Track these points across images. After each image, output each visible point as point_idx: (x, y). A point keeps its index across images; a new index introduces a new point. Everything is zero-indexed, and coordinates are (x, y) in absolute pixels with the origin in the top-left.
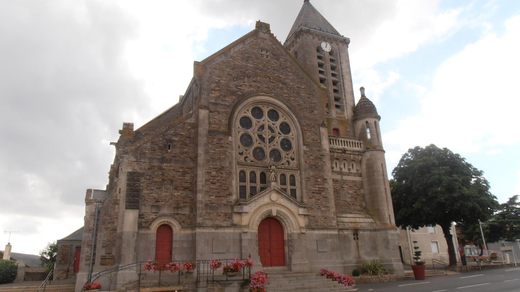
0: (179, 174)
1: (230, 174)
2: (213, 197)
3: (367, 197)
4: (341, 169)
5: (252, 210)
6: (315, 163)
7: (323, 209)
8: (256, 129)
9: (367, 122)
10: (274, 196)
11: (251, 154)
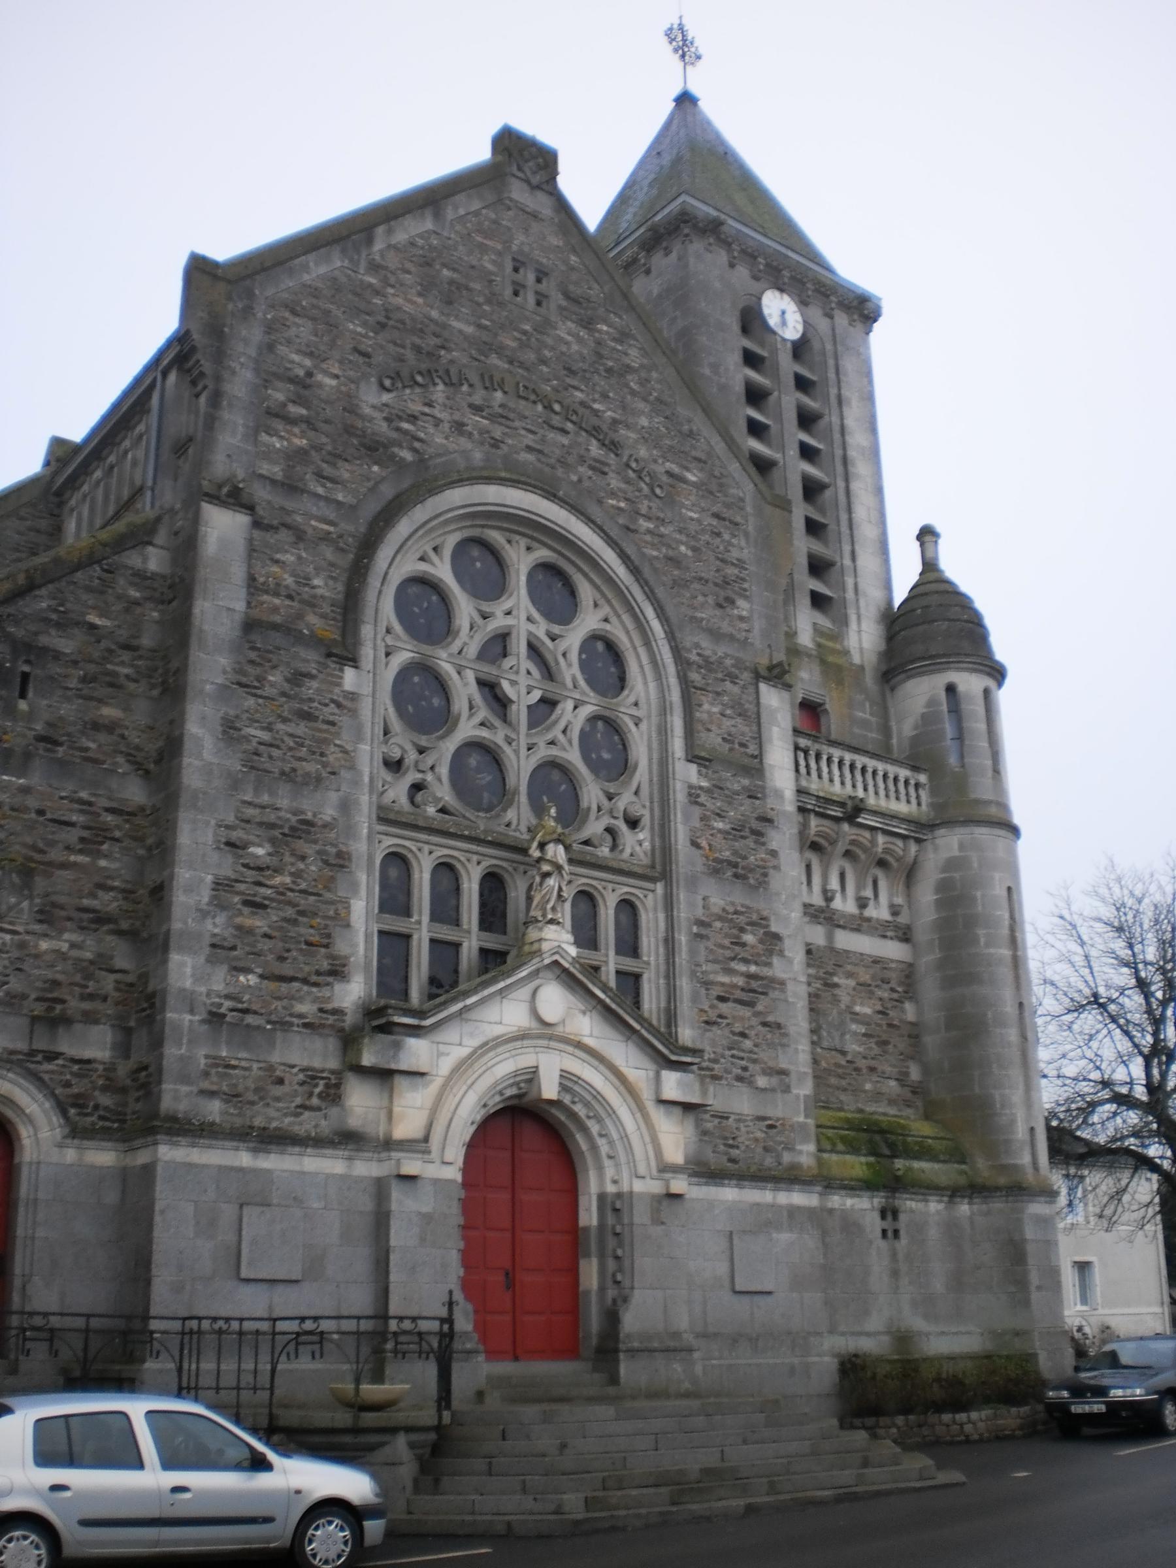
0: (71, 836)
1: (340, 862)
2: (253, 979)
3: (930, 1041)
4: (828, 897)
5: (445, 1067)
6: (735, 853)
7: (762, 1082)
8: (473, 650)
9: (951, 689)
10: (554, 1000)
11: (444, 770)
